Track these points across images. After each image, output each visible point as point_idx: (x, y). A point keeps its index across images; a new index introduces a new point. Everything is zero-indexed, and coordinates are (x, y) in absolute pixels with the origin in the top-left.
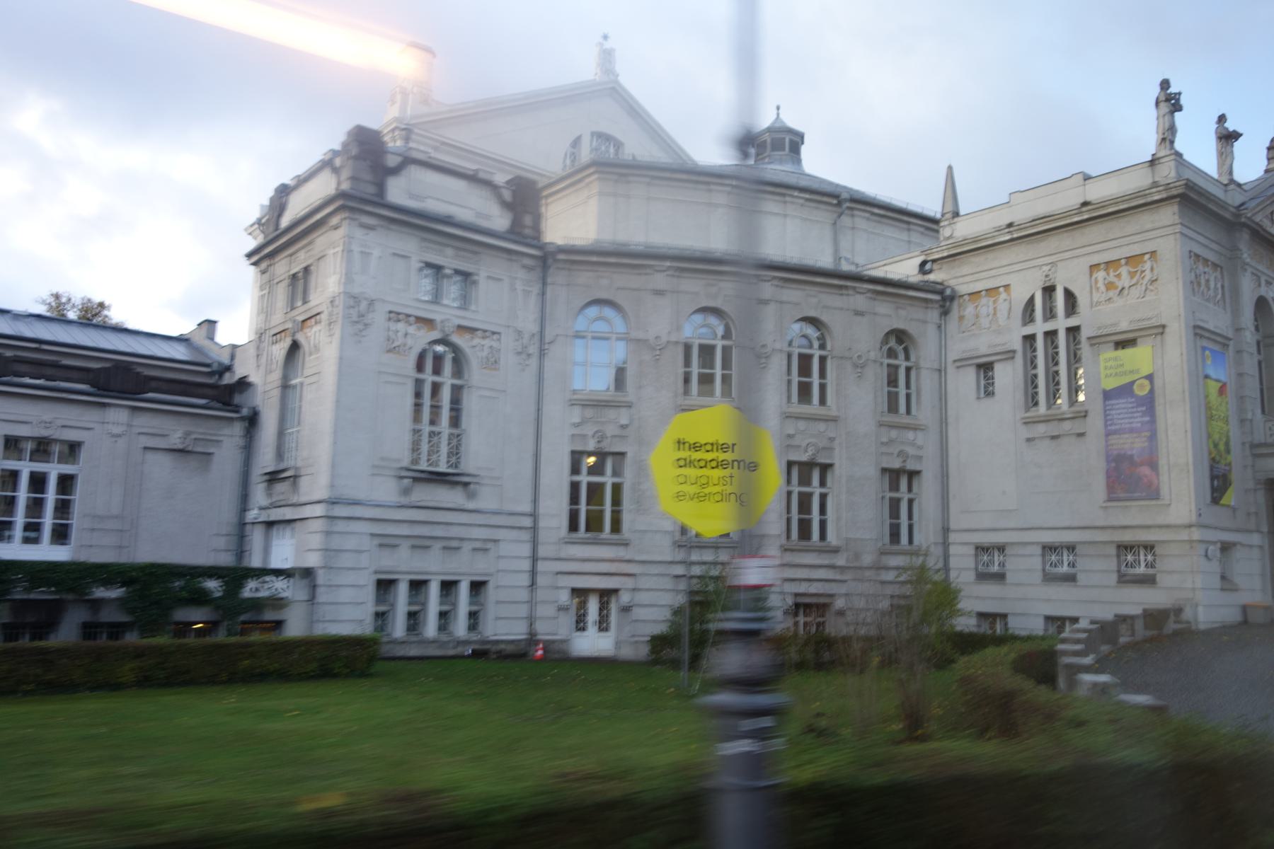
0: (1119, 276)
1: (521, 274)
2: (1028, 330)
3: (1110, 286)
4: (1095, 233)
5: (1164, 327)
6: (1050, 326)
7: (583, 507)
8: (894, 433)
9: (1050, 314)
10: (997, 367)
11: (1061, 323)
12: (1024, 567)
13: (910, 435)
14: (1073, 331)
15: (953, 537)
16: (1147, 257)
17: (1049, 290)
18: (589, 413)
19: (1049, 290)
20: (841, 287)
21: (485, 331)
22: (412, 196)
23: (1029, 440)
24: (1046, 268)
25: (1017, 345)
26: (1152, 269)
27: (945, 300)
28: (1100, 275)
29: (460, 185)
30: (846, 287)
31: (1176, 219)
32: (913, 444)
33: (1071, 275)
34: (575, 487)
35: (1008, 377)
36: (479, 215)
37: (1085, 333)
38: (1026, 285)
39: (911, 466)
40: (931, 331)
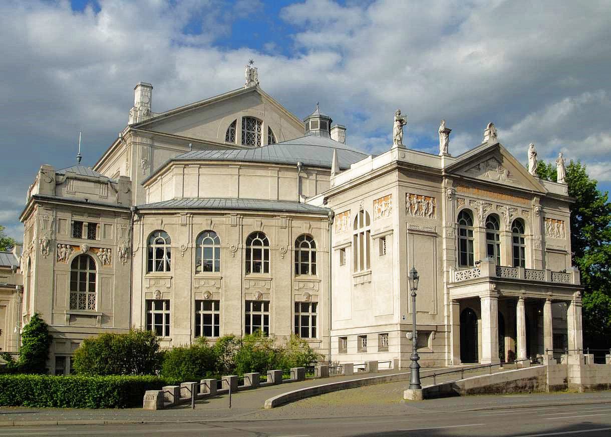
0: (381, 206)
4: (375, 183)
5: (393, 230)
7: (164, 324)
8: (301, 285)
9: (362, 226)
10: (346, 250)
12: (352, 344)
13: (311, 285)
14: (369, 231)
15: (333, 333)
16: (389, 196)
18: (153, 282)
19: (362, 212)
20: (273, 216)
21: (103, 249)
23: (355, 285)
24: (360, 202)
26: (391, 202)
27: (330, 217)
28: (376, 205)
29: (92, 184)
30: (275, 216)
31: (397, 179)
32: (313, 289)
33: (368, 206)
34: (297, 318)
35: (349, 253)
36: (101, 197)
37: (372, 233)
38: (355, 211)
39: (313, 300)
40: (324, 233)
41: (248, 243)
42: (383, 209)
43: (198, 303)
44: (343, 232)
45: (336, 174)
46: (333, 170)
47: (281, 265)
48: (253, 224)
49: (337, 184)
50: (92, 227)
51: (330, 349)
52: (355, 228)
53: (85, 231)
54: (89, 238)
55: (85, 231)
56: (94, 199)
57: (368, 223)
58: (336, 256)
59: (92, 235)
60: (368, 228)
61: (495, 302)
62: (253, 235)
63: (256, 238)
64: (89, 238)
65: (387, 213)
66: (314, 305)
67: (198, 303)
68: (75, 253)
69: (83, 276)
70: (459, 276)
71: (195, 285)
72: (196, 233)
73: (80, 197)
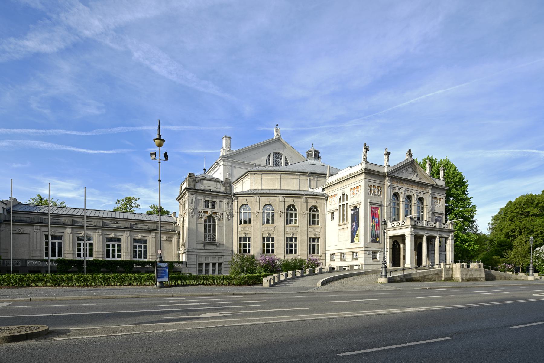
1: (227, 200)
2: (340, 204)
3: (353, 193)
6: (343, 203)
8: (312, 229)
9: (343, 201)
11: (345, 203)
13: (317, 230)
14: (347, 204)
17: (344, 194)
18: (242, 229)
19: (344, 194)
22: (202, 187)
25: (338, 208)
27: (326, 197)
29: (213, 183)
33: (347, 192)
35: (336, 214)
36: (217, 188)
37: (349, 204)
38: (340, 194)
39: (318, 237)
40: (323, 205)
41: (287, 209)
42: (355, 193)
43: (264, 238)
44: (333, 204)
45: (329, 176)
46: (328, 175)
47: (302, 221)
48: (289, 201)
49: (329, 182)
50: (214, 203)
51: (325, 259)
52: (340, 202)
53: (210, 205)
54: (212, 208)
55: (210, 205)
56: (214, 189)
57: (347, 200)
58: (329, 216)
59: (213, 207)
60: (347, 202)
61: (413, 238)
62: (289, 206)
63: (291, 207)
64: (212, 208)
65: (358, 195)
66: (318, 239)
67: (264, 238)
68: (206, 215)
69: (210, 226)
70: (393, 225)
71: (286, 230)
72: (263, 205)
73: (207, 188)
